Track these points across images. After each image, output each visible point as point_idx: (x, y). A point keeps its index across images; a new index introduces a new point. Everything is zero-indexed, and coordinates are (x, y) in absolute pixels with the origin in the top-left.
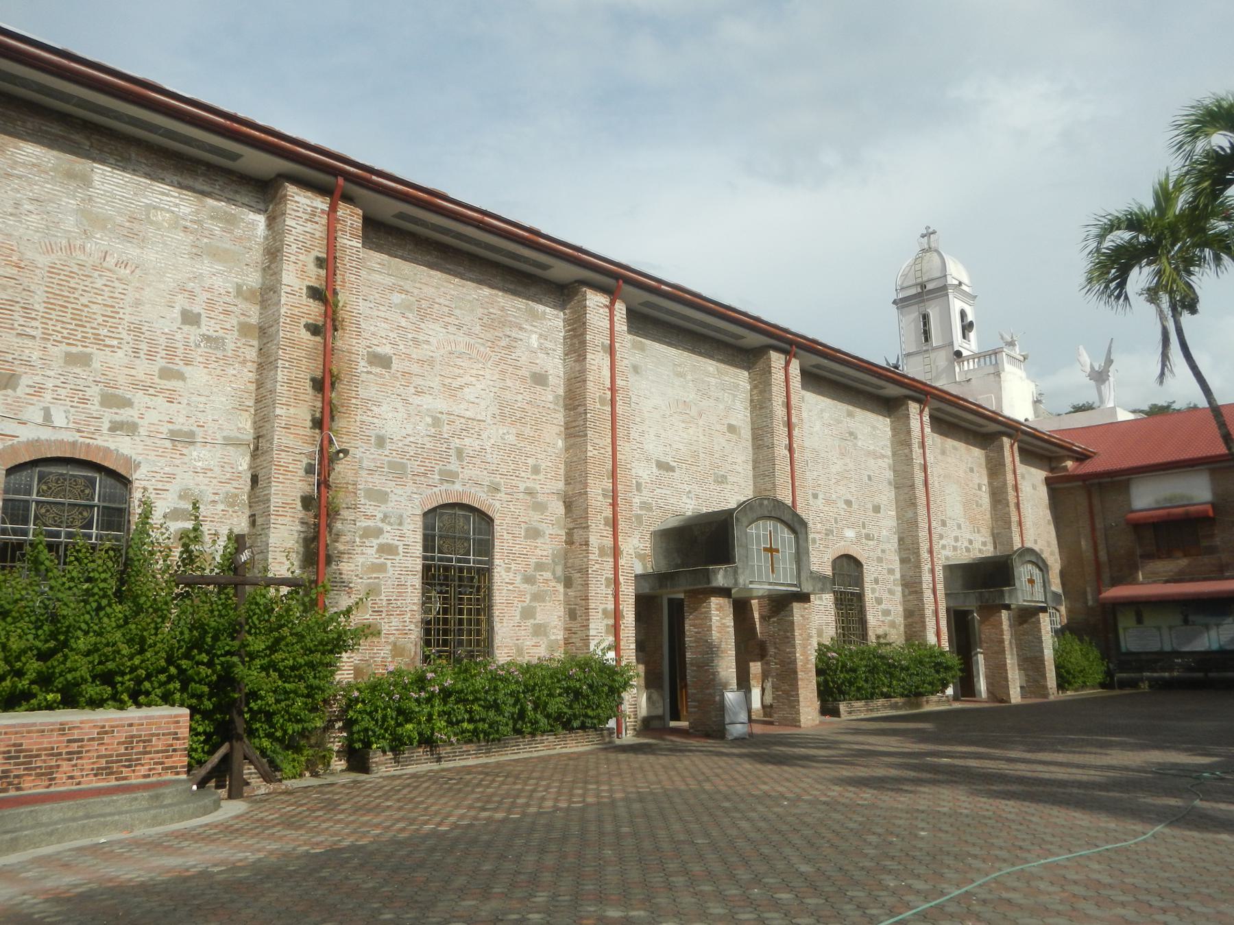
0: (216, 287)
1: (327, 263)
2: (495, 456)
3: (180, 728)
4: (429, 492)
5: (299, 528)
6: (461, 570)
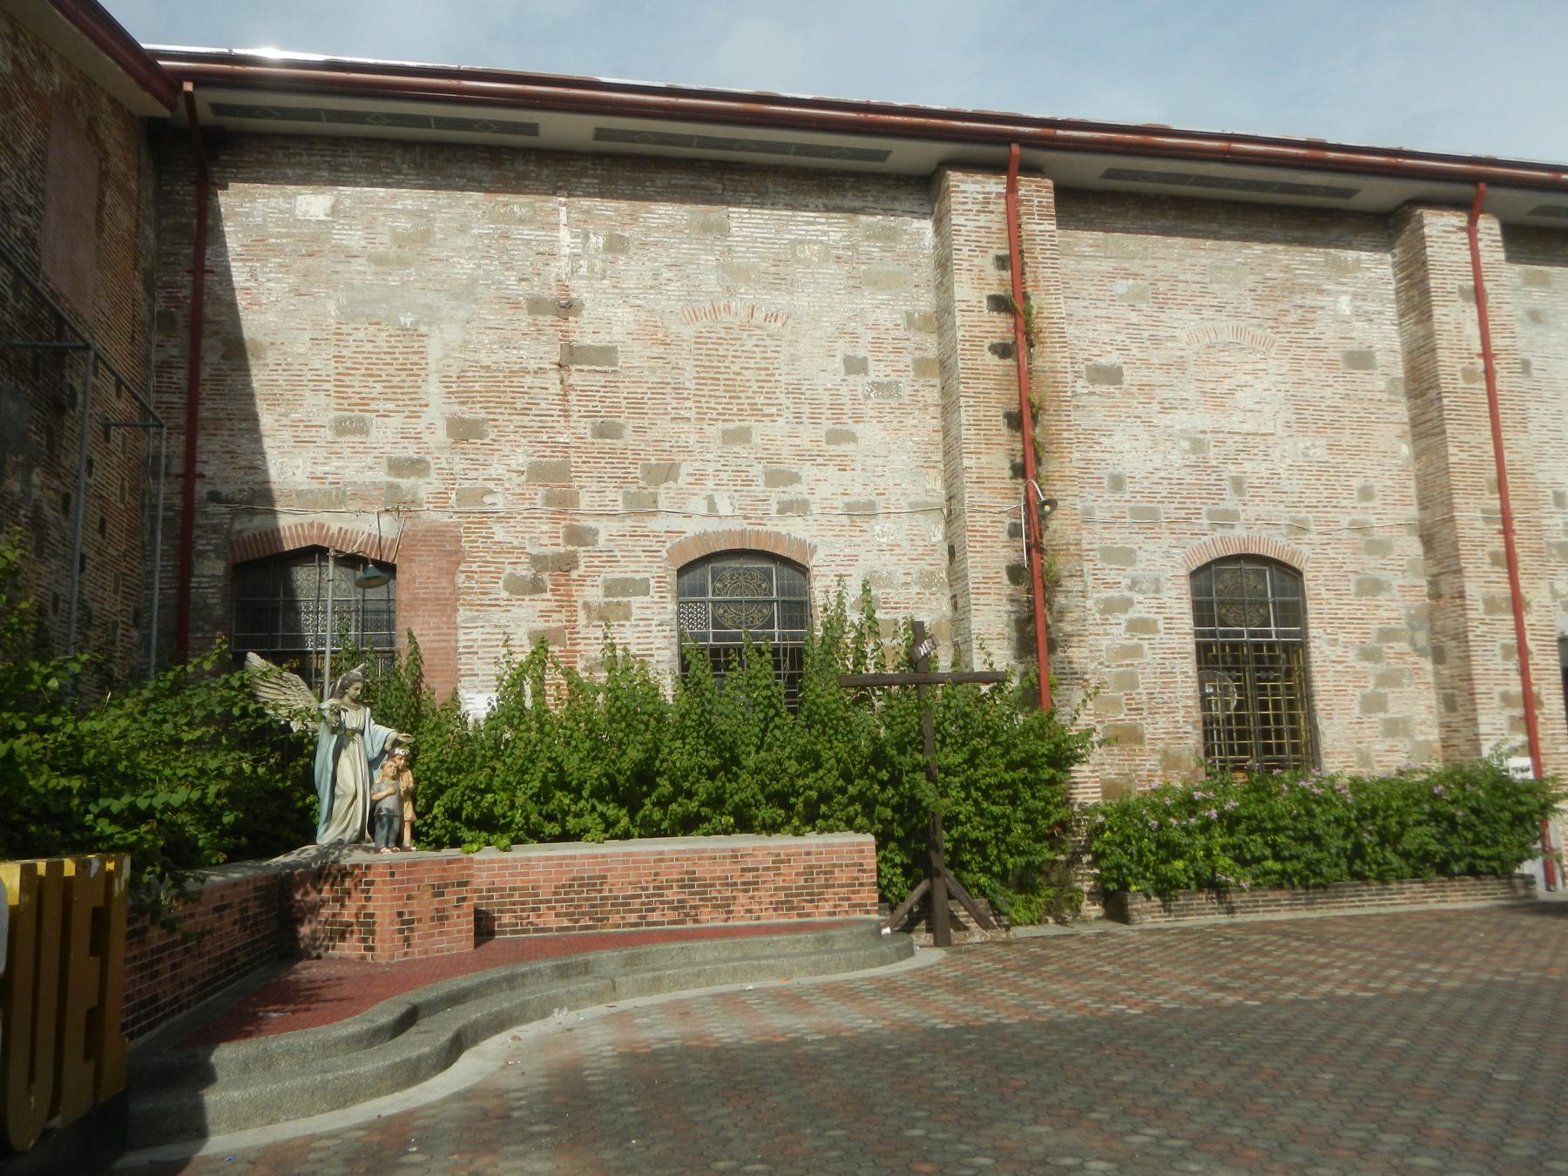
0: (881, 321)
1: (1013, 261)
2: (1294, 482)
3: (864, 858)
4: (1196, 543)
5: (1008, 607)
6: (1258, 646)
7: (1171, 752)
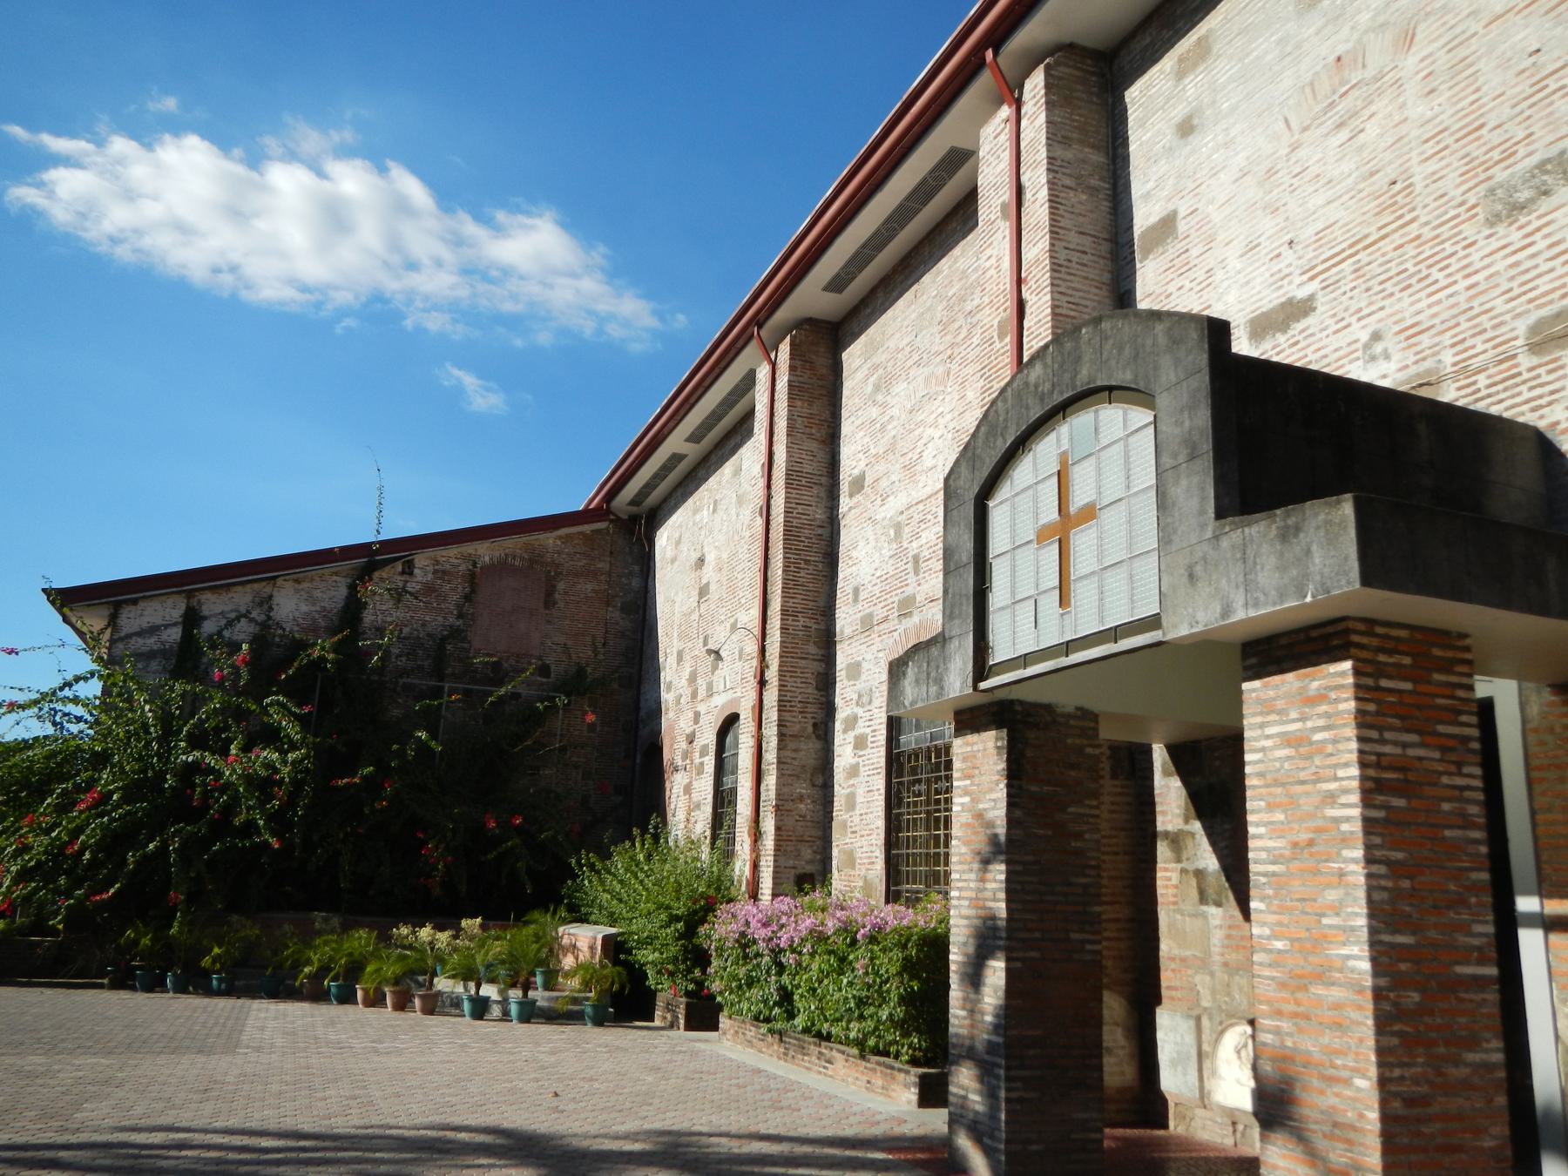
4: (892, 640)
7: (869, 877)
